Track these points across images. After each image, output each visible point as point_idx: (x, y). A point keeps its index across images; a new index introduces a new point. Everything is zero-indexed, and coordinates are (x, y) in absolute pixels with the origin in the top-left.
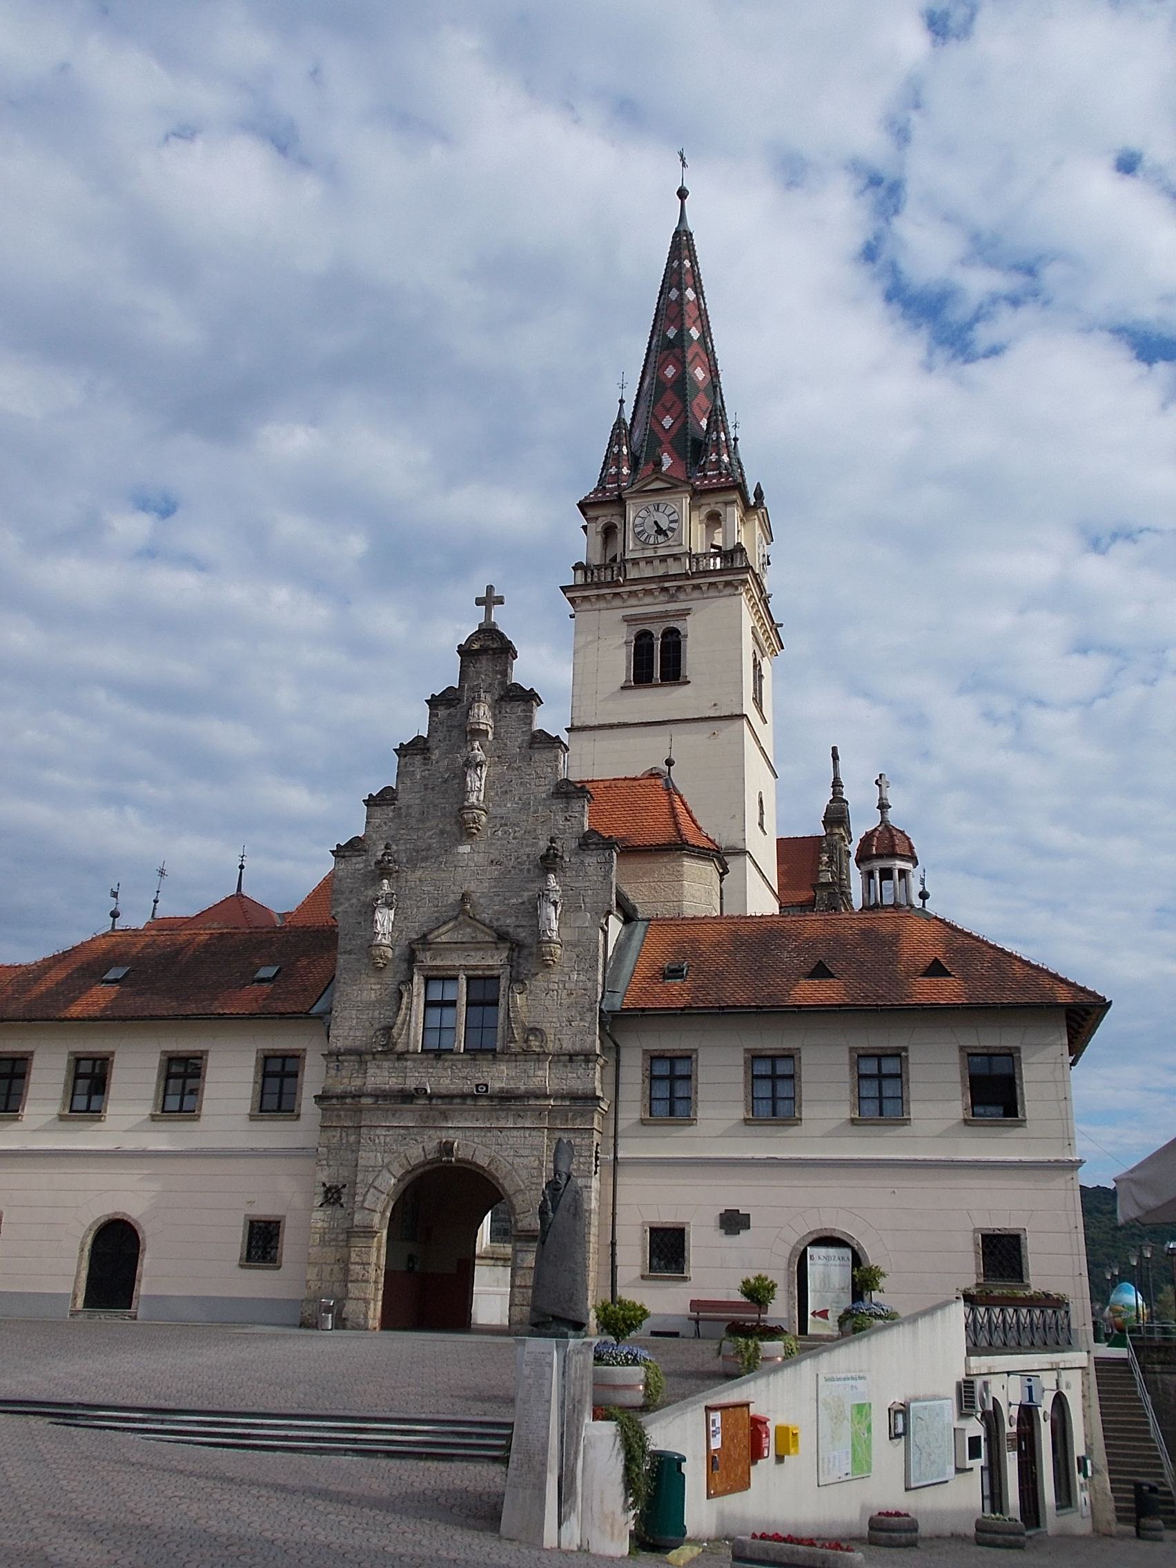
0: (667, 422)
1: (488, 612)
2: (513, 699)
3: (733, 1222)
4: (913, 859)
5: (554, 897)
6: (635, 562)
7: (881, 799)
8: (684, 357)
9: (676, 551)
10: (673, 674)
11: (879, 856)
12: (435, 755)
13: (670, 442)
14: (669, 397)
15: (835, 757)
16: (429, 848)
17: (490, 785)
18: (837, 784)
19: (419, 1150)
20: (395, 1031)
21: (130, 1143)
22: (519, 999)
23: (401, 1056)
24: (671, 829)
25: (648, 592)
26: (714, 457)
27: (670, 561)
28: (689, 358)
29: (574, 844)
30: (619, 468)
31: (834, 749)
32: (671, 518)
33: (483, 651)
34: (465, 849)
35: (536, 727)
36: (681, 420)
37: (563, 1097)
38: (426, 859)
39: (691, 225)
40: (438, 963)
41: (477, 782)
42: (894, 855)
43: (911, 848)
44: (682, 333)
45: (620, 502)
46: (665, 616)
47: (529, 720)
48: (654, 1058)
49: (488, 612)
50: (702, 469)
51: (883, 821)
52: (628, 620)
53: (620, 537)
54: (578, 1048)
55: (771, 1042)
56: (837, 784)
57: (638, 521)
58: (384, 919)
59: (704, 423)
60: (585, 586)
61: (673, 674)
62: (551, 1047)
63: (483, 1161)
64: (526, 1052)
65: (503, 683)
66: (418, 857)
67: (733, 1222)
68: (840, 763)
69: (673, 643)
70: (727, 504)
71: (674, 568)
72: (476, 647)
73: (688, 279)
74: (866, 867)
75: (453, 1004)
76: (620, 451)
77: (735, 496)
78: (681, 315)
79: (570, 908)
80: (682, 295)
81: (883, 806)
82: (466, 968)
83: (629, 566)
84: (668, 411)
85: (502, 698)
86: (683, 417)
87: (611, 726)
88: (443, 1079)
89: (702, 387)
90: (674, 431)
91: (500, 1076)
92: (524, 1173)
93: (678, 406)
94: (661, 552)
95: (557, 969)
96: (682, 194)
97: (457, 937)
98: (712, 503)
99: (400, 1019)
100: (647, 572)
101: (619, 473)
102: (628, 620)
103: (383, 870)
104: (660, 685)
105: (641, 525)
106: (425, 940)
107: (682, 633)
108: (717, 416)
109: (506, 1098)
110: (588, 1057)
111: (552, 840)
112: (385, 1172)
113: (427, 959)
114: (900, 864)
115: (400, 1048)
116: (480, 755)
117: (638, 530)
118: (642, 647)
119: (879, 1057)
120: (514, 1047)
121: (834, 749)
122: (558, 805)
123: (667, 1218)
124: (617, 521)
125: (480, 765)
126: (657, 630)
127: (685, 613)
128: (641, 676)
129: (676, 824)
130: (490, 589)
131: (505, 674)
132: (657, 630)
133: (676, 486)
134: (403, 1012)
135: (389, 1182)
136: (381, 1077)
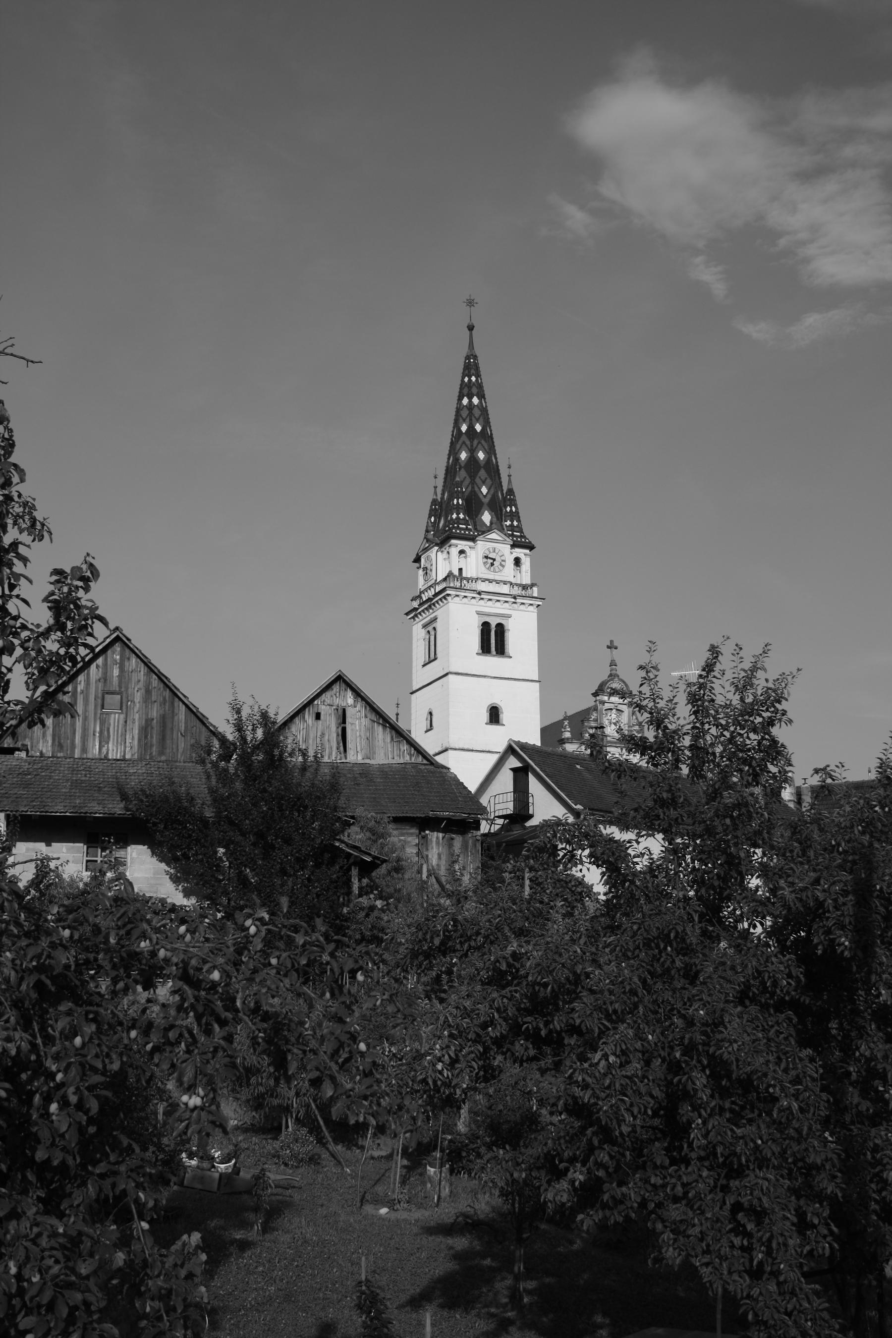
0: (484, 490)
10: (501, 650)
14: (482, 473)
36: (492, 491)
39: (478, 351)
52: (478, 613)
61: (501, 650)
84: (484, 482)
90: (489, 496)
96: (471, 328)
102: (478, 613)
104: (494, 656)
107: (506, 628)
126: (493, 622)
130: (612, 642)
132: (493, 622)
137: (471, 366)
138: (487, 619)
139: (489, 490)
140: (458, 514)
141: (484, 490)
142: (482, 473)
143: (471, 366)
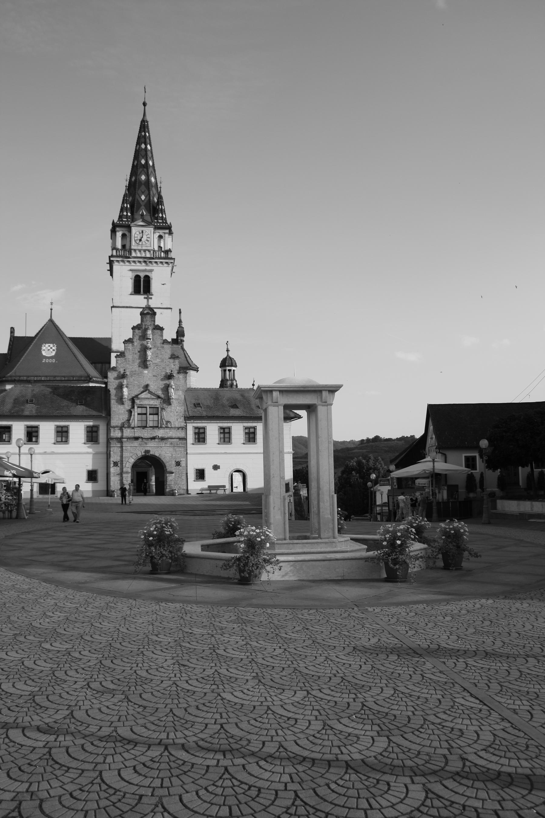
0: (143, 197)
1: (148, 301)
2: (158, 329)
3: (216, 467)
4: (236, 366)
5: (174, 387)
6: (135, 250)
7: (227, 348)
8: (148, 173)
9: (149, 248)
11: (228, 366)
12: (135, 344)
13: (145, 206)
14: (143, 188)
15: (180, 313)
16: (135, 371)
17: (153, 354)
18: (180, 322)
19: (140, 453)
20: (131, 421)
21: (48, 451)
22: (164, 413)
23: (133, 428)
24: (186, 362)
25: (140, 262)
26: (160, 215)
27: (147, 252)
28: (150, 173)
29: (176, 372)
30: (127, 213)
31: (180, 310)
32: (148, 236)
33: (148, 314)
34: (146, 372)
35: (164, 338)
36: (148, 198)
37: (177, 439)
38: (135, 374)
39: (148, 118)
40: (141, 403)
41: (149, 353)
42: (232, 366)
43: (236, 364)
44: (147, 162)
45: (129, 228)
46: (145, 271)
47: (162, 336)
48: (196, 428)
49: (148, 301)
50: (157, 219)
51: (228, 355)
53: (128, 239)
54: (180, 426)
55: (225, 425)
56: (180, 322)
57: (136, 235)
58: (125, 390)
59: (156, 200)
60: (117, 256)
62: (173, 426)
63: (157, 455)
64: (167, 427)
65: (154, 324)
66: (133, 373)
67: (216, 467)
68: (182, 314)
69: (147, 279)
70: (165, 233)
71: (148, 255)
72: (145, 312)
73: (148, 140)
74: (224, 368)
75: (146, 414)
76: (127, 206)
77: (167, 231)
78: (146, 155)
79: (176, 390)
80: (146, 147)
81: (228, 351)
82: (149, 405)
83: (132, 251)
84: (143, 193)
85: (154, 329)
86: (148, 195)
87: (127, 307)
88: (146, 433)
89: (153, 185)
91: (160, 433)
92: (168, 458)
93: (147, 192)
94: (144, 248)
95: (173, 405)
96: (145, 104)
97: (146, 397)
98: (161, 232)
99: (132, 418)
100: (139, 255)
101: (127, 215)
103: (123, 376)
105: (137, 237)
106: (137, 396)
108: (160, 197)
109: (163, 439)
110: (182, 428)
111: (172, 371)
112: (131, 458)
113: (137, 402)
114: (233, 368)
115: (132, 425)
116: (149, 345)
117: (136, 239)
118: (137, 279)
119: (249, 428)
120: (164, 426)
121: (180, 310)
122: (172, 360)
123: (200, 467)
124: (127, 233)
125: (150, 349)
126: (142, 275)
127: (151, 271)
128: (137, 291)
129: (187, 360)
131: (154, 321)
132: (142, 275)
133: (149, 225)
134: (132, 417)
135: (132, 461)
136: (128, 433)
137: (144, 126)
138: (138, 274)
139: (146, 197)
140: (127, 213)
141: (143, 197)
142: (143, 188)
143: (144, 126)
